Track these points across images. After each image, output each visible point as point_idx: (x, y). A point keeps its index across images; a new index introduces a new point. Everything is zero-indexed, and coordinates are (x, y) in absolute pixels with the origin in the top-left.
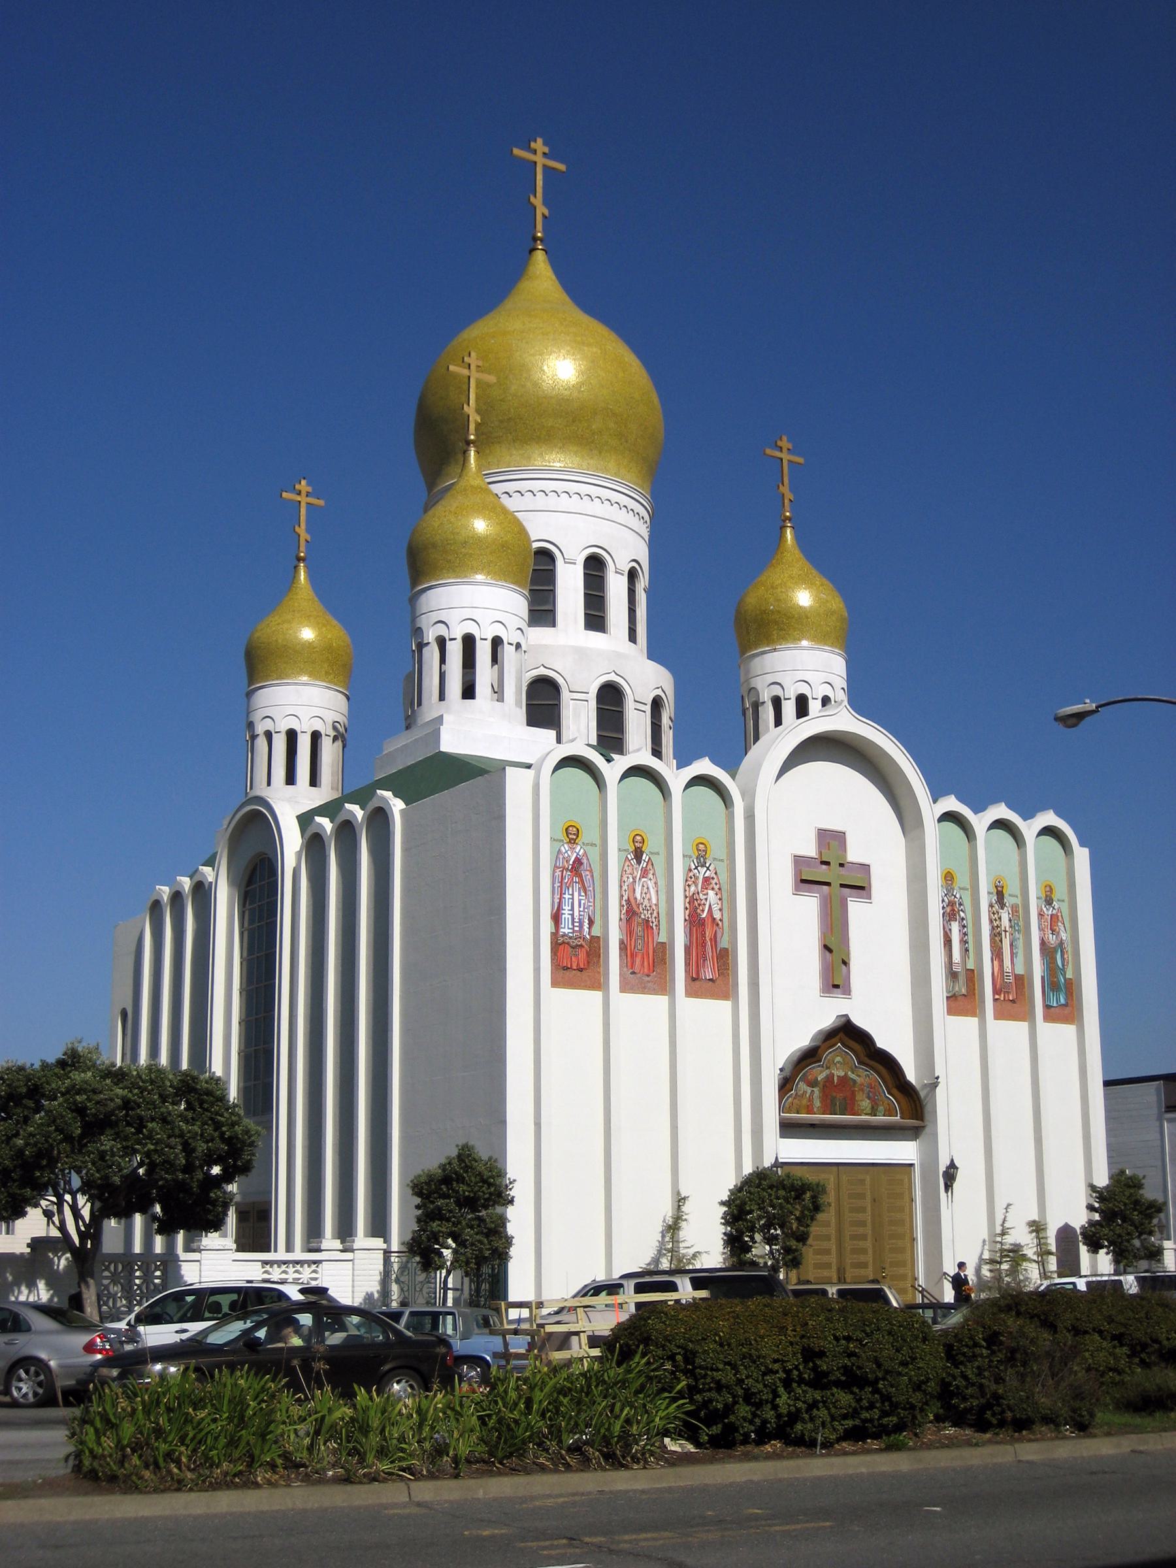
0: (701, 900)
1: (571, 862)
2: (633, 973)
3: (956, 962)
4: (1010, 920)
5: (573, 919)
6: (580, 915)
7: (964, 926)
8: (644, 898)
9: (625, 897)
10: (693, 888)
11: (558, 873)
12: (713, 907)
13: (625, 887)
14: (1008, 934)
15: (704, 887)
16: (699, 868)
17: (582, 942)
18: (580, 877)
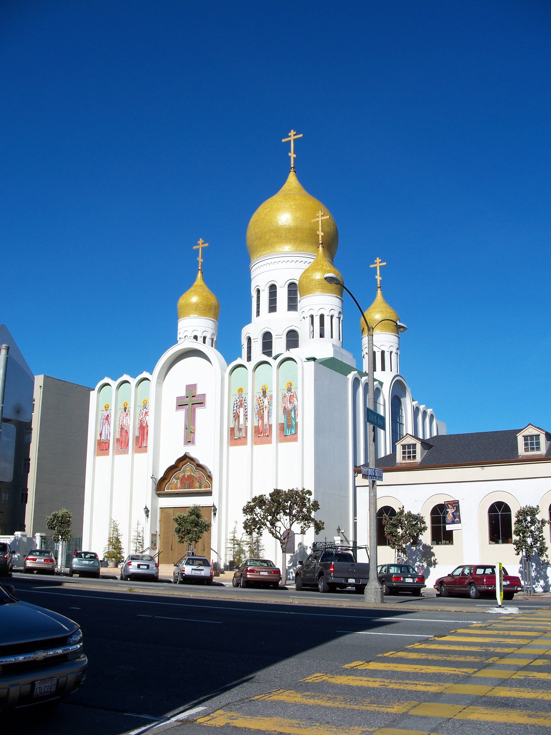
1: (106, 417)
2: (121, 448)
4: (269, 402)
7: (246, 409)
9: (120, 424)
10: (142, 416)
11: (102, 421)
13: (121, 421)
14: (267, 408)
15: (145, 415)
17: (107, 441)
18: (108, 421)
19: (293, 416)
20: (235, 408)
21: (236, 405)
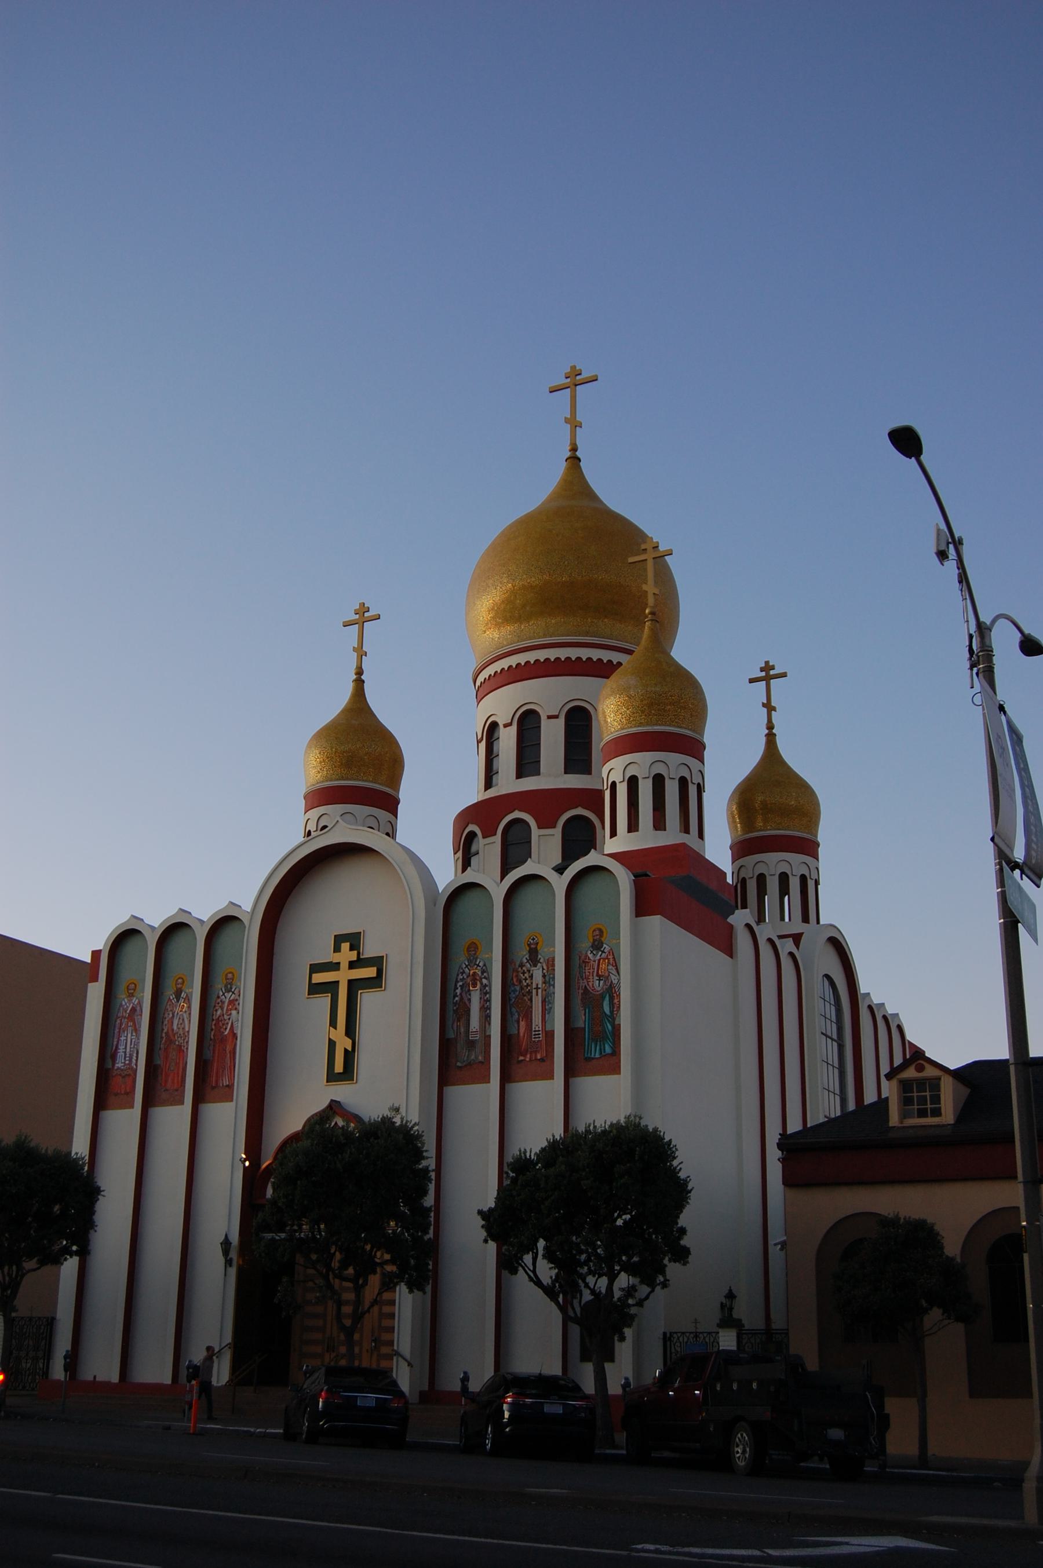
0: (225, 1020)
1: (128, 1012)
3: (474, 1030)
4: (544, 976)
5: (125, 1054)
6: (130, 1051)
7: (486, 993)
8: (179, 1028)
9: (165, 1030)
10: (219, 1012)
12: (234, 1024)
13: (166, 1022)
14: (540, 991)
16: (226, 994)
19: (607, 1009)
20: (458, 991)
21: (461, 983)
